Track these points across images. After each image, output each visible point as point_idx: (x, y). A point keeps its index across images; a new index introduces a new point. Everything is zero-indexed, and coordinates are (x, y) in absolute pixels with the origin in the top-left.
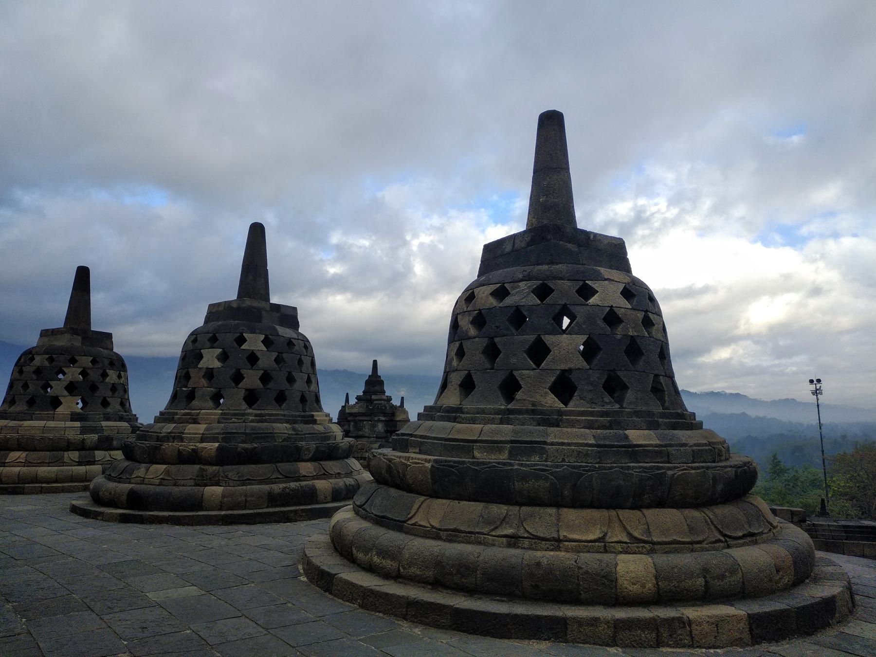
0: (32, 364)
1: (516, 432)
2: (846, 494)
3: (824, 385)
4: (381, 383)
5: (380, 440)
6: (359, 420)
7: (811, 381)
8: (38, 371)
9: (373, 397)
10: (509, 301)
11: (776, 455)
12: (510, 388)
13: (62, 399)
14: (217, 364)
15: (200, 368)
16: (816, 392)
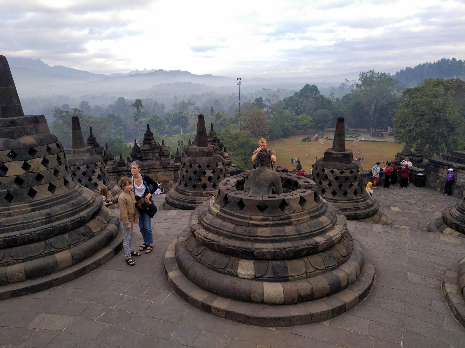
1: (353, 205)
2: (247, 127)
3: (242, 81)
4: (152, 134)
5: (158, 160)
6: (147, 152)
7: (238, 79)
8: (84, 174)
9: (152, 142)
10: (344, 175)
11: (213, 107)
12: (345, 194)
13: (97, 183)
14: (212, 175)
15: (206, 177)
16: (239, 84)
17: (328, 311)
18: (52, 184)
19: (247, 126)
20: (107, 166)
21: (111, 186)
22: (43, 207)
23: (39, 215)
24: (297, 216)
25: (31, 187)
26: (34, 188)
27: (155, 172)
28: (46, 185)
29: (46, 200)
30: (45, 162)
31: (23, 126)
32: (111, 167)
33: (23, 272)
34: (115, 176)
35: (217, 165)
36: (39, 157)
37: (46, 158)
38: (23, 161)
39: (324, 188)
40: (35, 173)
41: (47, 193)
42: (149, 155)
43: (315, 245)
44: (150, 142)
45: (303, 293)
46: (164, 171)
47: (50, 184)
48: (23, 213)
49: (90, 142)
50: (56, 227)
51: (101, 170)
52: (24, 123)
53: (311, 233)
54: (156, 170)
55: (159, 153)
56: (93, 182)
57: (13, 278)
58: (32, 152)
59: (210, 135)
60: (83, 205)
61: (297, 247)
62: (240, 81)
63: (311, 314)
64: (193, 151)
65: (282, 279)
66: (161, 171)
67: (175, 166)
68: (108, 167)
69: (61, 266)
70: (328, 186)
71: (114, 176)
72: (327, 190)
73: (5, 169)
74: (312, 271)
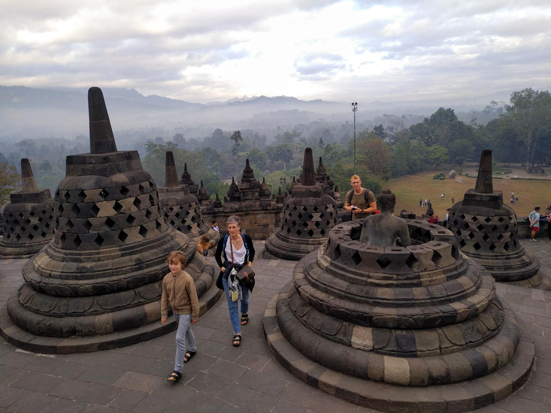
0: (173, 211)
2: (363, 162)
4: (252, 171)
5: (257, 200)
7: (353, 104)
8: (177, 215)
9: (251, 179)
10: (490, 223)
11: (322, 138)
12: (492, 247)
13: (191, 226)
14: (320, 219)
15: (313, 222)
16: (354, 110)
17: (470, 400)
18: (143, 226)
19: (364, 159)
20: (203, 206)
21: (206, 229)
22: (133, 252)
23: (129, 261)
24: (429, 276)
25: (122, 230)
26: (125, 231)
27: (254, 214)
28: (137, 227)
29: (137, 244)
30: (137, 202)
31: (116, 162)
32: (206, 207)
33: (111, 323)
34: (210, 218)
35: (327, 208)
36: (130, 197)
37: (138, 197)
39: (463, 240)
40: (126, 215)
41: (138, 236)
42: (248, 194)
43: (452, 314)
44: (249, 180)
45: (435, 374)
46: (264, 213)
47: (142, 226)
48: (113, 258)
49: (185, 180)
50: (146, 274)
51: (195, 211)
53: (448, 298)
54: (255, 212)
55: (259, 192)
56: (186, 224)
57: (101, 329)
58: (124, 191)
59: (318, 171)
61: (429, 314)
62: (356, 106)
63: (446, 402)
64: (298, 190)
65: (409, 354)
66: (261, 214)
67: (276, 208)
68: (203, 208)
69: (149, 319)
70: (468, 236)
71: (209, 218)
72: (468, 241)
73: (97, 209)
74: (448, 346)
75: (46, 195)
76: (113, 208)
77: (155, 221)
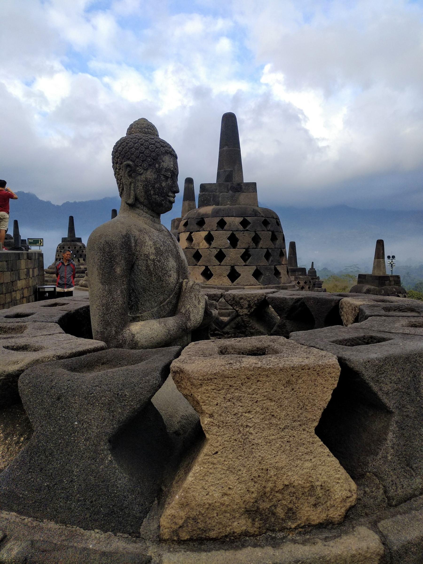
28: (201, 267)
30: (209, 239)
31: (214, 193)
37: (212, 233)
38: (189, 233)
40: (194, 250)
47: (207, 267)
52: (216, 189)
60: (228, 309)
75: (390, 280)
76: (186, 240)
77: (229, 268)
